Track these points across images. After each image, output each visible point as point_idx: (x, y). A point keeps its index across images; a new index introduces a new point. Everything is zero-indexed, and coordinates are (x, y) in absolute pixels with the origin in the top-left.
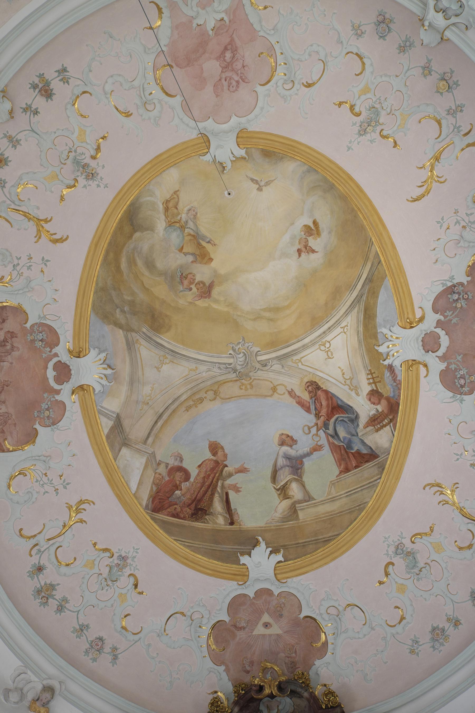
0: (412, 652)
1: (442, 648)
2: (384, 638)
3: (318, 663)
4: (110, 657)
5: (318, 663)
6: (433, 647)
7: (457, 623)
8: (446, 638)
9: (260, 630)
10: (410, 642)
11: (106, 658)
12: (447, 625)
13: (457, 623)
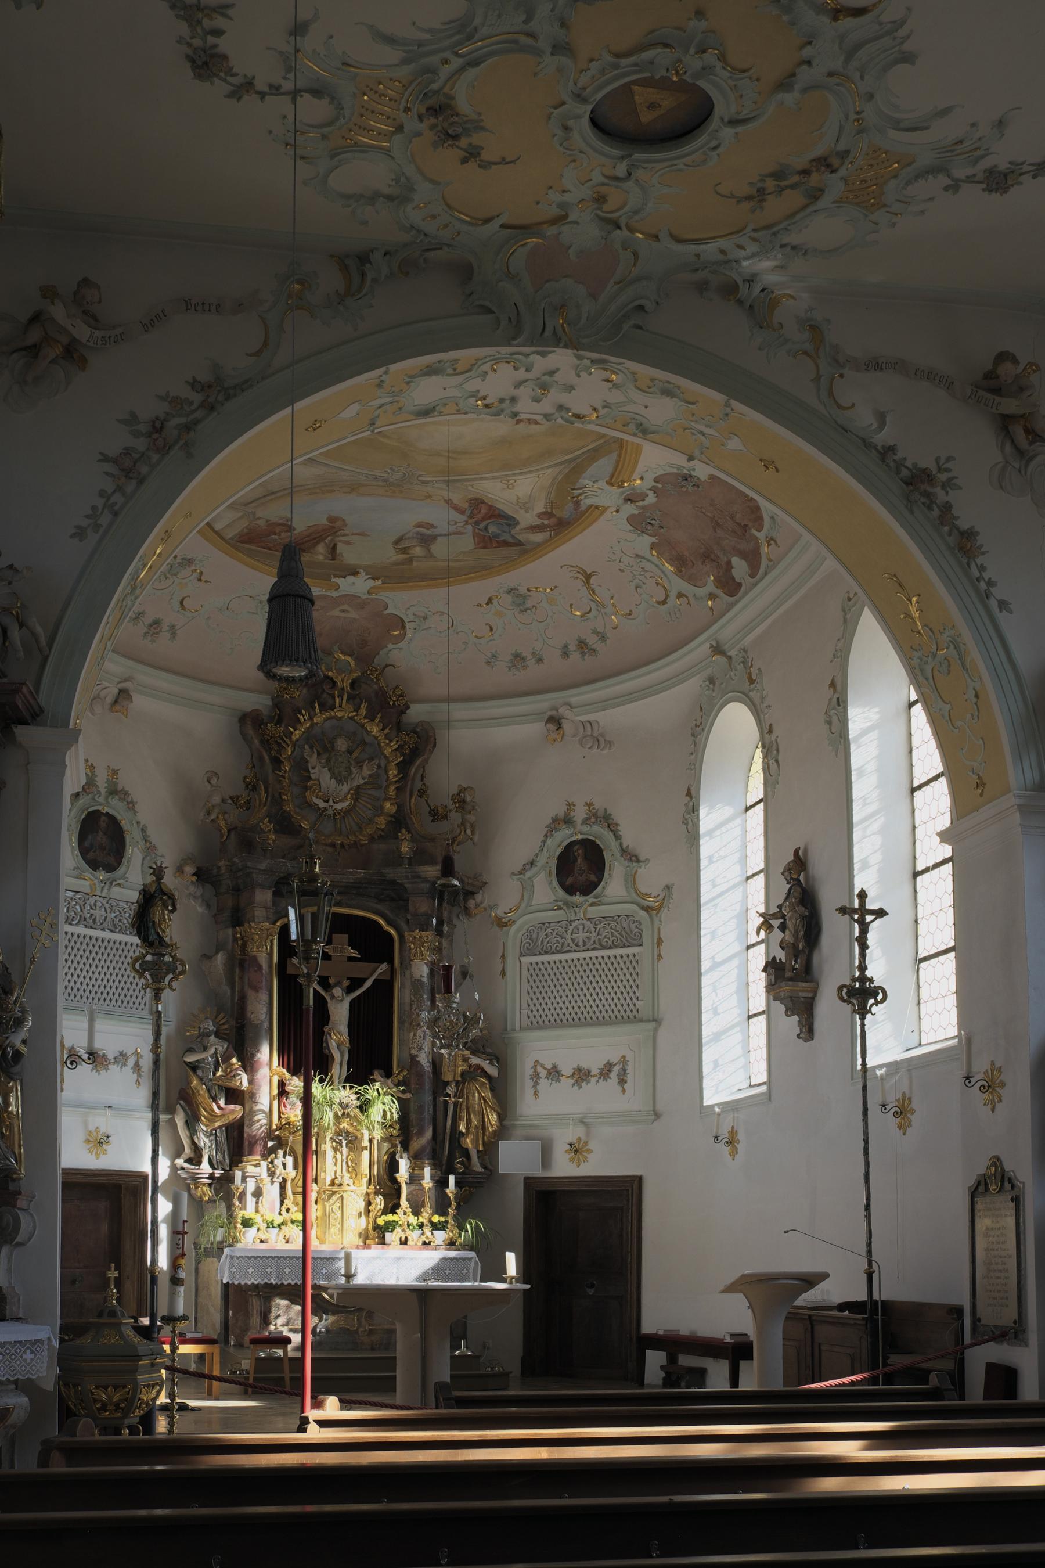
0: (488, 663)
1: (517, 673)
2: (466, 643)
3: (390, 646)
5: (390, 646)
6: (510, 668)
7: (540, 660)
8: (525, 667)
10: (490, 655)
12: (529, 657)
13: (540, 660)
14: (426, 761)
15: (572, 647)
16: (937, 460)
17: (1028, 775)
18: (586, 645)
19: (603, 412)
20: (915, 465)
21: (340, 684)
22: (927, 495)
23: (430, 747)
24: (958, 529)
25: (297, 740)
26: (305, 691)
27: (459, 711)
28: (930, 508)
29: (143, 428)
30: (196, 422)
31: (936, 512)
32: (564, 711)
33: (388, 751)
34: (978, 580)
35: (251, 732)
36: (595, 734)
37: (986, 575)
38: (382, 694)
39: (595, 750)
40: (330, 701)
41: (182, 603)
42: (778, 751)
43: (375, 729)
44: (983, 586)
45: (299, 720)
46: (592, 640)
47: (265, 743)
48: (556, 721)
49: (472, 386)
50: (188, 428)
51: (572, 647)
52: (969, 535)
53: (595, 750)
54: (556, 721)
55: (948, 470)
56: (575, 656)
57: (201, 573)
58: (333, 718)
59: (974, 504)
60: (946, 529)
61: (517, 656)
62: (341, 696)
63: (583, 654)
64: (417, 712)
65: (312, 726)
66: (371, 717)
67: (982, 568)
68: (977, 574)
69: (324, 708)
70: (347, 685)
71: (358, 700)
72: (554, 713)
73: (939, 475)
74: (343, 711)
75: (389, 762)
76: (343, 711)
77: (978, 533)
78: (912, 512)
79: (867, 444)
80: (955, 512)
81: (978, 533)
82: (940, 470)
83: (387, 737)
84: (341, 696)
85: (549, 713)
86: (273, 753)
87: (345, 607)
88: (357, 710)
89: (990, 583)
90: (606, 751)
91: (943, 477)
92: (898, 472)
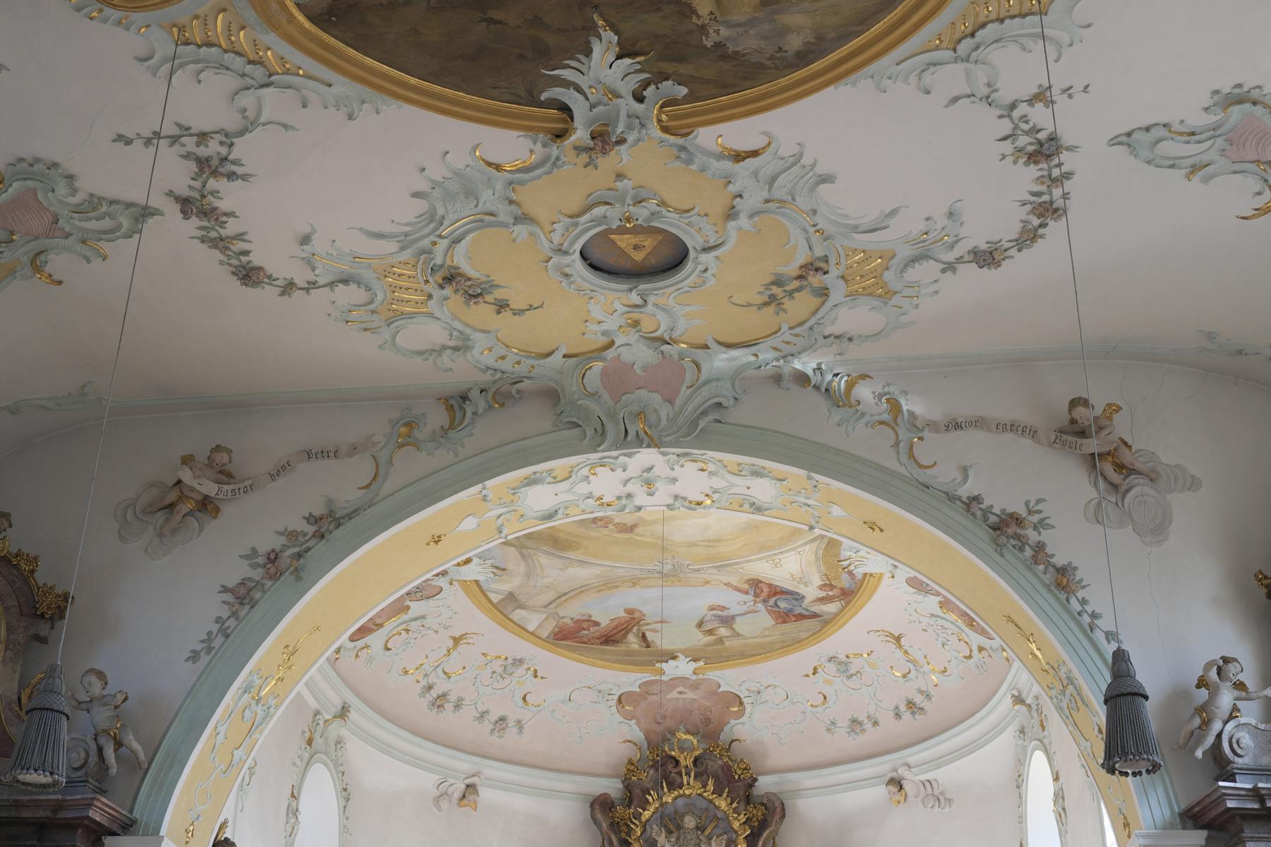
3: (733, 722)
4: (515, 730)
5: (733, 722)
7: (876, 723)
8: (864, 731)
9: (674, 694)
11: (512, 731)
12: (866, 721)
13: (876, 723)
14: (776, 832)
15: (903, 708)
16: (1027, 504)
17: (1157, 812)
18: (915, 704)
19: (716, 496)
20: (1003, 511)
21: (683, 763)
22: (1017, 537)
23: (777, 817)
24: (1054, 566)
25: (648, 821)
26: (652, 772)
27: (807, 780)
28: (1021, 549)
29: (261, 560)
30: (308, 550)
31: (1028, 552)
32: (903, 771)
33: (736, 825)
34: (1079, 614)
35: (599, 816)
36: (936, 793)
37: (1089, 609)
38: (727, 769)
39: (936, 809)
40: (678, 779)
41: (524, 699)
42: (1063, 798)
43: (722, 803)
44: (1086, 619)
45: (648, 801)
46: (918, 699)
47: (615, 826)
48: (897, 783)
49: (583, 488)
50: (299, 556)
51: (903, 708)
52: (1062, 571)
53: (936, 809)
54: (897, 783)
55: (1039, 512)
56: (907, 716)
57: (536, 671)
58: (681, 796)
59: (1069, 540)
60: (1042, 567)
61: (855, 721)
62: (688, 774)
63: (913, 713)
64: (765, 784)
65: (662, 805)
66: (718, 791)
67: (1084, 602)
68: (1079, 608)
69: (672, 786)
70: (690, 762)
71: (705, 777)
72: (894, 774)
73: (1030, 518)
74: (691, 787)
75: (738, 836)
76: (691, 787)
77: (1075, 569)
78: (1002, 556)
79: (952, 498)
80: (1049, 550)
81: (1075, 569)
82: (1030, 513)
83: (735, 810)
84: (688, 774)
85: (890, 775)
86: (623, 835)
87: (681, 689)
88: (705, 786)
89: (1094, 616)
90: (947, 809)
91: (1035, 518)
92: (986, 519)
